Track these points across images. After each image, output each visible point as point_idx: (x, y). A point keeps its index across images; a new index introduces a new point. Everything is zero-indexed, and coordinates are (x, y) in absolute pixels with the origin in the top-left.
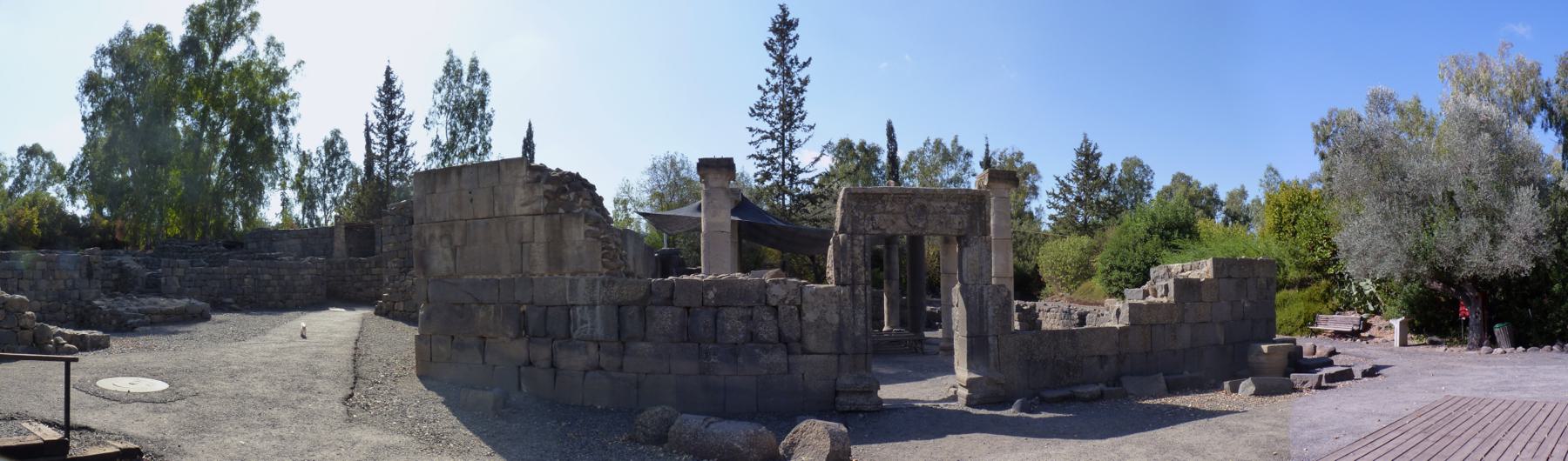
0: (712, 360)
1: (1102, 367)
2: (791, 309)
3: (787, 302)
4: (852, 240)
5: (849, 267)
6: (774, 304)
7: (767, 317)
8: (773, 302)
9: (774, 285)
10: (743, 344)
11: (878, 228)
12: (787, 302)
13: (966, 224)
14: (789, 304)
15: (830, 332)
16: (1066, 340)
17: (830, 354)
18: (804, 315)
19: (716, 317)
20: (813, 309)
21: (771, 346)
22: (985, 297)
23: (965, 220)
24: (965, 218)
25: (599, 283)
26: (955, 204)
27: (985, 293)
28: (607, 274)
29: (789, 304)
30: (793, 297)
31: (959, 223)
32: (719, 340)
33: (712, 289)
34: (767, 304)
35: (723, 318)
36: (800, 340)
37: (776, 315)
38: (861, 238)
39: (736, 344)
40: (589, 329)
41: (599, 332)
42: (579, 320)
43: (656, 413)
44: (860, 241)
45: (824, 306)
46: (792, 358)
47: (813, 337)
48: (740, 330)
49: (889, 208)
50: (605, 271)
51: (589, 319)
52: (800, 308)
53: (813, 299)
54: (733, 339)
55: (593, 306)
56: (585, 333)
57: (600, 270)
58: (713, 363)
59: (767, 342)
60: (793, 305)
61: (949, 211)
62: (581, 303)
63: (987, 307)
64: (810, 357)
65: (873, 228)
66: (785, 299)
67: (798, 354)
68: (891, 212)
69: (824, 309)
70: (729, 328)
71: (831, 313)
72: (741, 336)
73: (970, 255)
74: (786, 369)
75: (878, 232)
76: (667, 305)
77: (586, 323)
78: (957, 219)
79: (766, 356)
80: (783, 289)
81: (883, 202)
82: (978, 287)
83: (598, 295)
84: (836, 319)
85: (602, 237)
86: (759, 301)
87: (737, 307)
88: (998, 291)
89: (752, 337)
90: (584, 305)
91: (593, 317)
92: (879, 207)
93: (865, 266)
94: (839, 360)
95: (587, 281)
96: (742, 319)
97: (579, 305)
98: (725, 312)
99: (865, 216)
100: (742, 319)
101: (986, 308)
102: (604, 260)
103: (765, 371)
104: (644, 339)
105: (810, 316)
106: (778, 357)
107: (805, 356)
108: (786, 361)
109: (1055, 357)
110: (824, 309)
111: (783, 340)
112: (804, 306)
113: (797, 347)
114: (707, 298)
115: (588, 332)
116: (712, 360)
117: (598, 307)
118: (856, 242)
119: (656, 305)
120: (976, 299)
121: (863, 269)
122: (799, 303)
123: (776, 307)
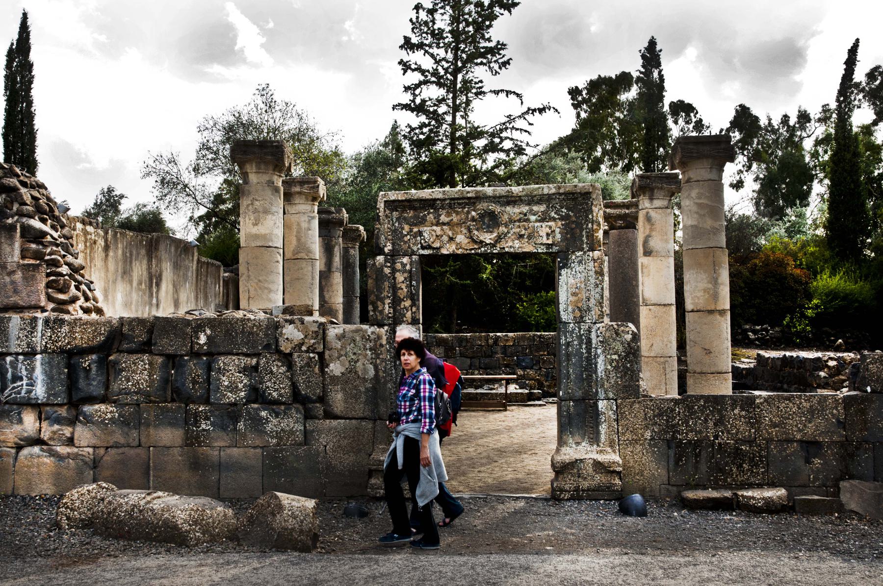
1: (808, 461)
2: (310, 358)
3: (304, 348)
4: (394, 263)
5: (388, 301)
6: (288, 351)
7: (278, 368)
8: (285, 347)
9: (287, 325)
10: (244, 405)
11: (429, 247)
12: (304, 348)
13: (558, 236)
14: (307, 351)
15: (362, 389)
16: (736, 411)
17: (362, 419)
18: (328, 366)
19: (209, 369)
20: (338, 358)
21: (283, 407)
22: (594, 341)
23: (558, 230)
24: (557, 226)
25: (40, 323)
26: (542, 208)
27: (593, 335)
28: (53, 310)
29: (307, 351)
30: (312, 341)
31: (548, 235)
33: (204, 331)
34: (278, 351)
35: (220, 369)
36: (322, 399)
37: (290, 365)
38: (405, 260)
40: (25, 387)
41: (40, 391)
42: (9, 375)
43: (88, 491)
44: (404, 265)
45: (355, 354)
46: (310, 424)
47: (340, 396)
48: (240, 386)
49: (443, 218)
50: (51, 306)
51: (24, 373)
52: (321, 355)
53: (339, 345)
54: (231, 397)
55: (30, 354)
56: (20, 393)
57: (42, 304)
58: (204, 430)
59: (277, 402)
60: (313, 352)
61: (533, 218)
62: (13, 349)
63: (597, 356)
64: (334, 423)
65: (423, 248)
66: (302, 344)
68: (448, 224)
70: (226, 383)
71: (364, 364)
72: (243, 394)
73: (571, 281)
74: (300, 438)
75: (426, 252)
76: (143, 352)
77: (21, 379)
78: (543, 229)
79: (275, 421)
81: (436, 210)
82: (584, 327)
83: (39, 339)
84: (372, 372)
85: (47, 258)
86: (267, 347)
87: (237, 354)
88: (617, 334)
89: (256, 395)
90: (18, 354)
91: (32, 370)
92: (431, 217)
94: (374, 428)
95: (22, 319)
96: (245, 370)
97: (10, 354)
98: (222, 361)
99: (411, 231)
100: (245, 370)
101: (595, 358)
102: (50, 290)
103: (275, 441)
104: (104, 400)
105: (336, 368)
106: (292, 423)
108: (302, 428)
109: (716, 437)
111: (297, 397)
112: (327, 353)
113: (319, 409)
114: (199, 344)
115: (23, 392)
116: (204, 426)
117: (38, 357)
118: (398, 266)
119: (131, 352)
120: (580, 344)
121: (408, 303)
122: (320, 348)
123: (291, 354)
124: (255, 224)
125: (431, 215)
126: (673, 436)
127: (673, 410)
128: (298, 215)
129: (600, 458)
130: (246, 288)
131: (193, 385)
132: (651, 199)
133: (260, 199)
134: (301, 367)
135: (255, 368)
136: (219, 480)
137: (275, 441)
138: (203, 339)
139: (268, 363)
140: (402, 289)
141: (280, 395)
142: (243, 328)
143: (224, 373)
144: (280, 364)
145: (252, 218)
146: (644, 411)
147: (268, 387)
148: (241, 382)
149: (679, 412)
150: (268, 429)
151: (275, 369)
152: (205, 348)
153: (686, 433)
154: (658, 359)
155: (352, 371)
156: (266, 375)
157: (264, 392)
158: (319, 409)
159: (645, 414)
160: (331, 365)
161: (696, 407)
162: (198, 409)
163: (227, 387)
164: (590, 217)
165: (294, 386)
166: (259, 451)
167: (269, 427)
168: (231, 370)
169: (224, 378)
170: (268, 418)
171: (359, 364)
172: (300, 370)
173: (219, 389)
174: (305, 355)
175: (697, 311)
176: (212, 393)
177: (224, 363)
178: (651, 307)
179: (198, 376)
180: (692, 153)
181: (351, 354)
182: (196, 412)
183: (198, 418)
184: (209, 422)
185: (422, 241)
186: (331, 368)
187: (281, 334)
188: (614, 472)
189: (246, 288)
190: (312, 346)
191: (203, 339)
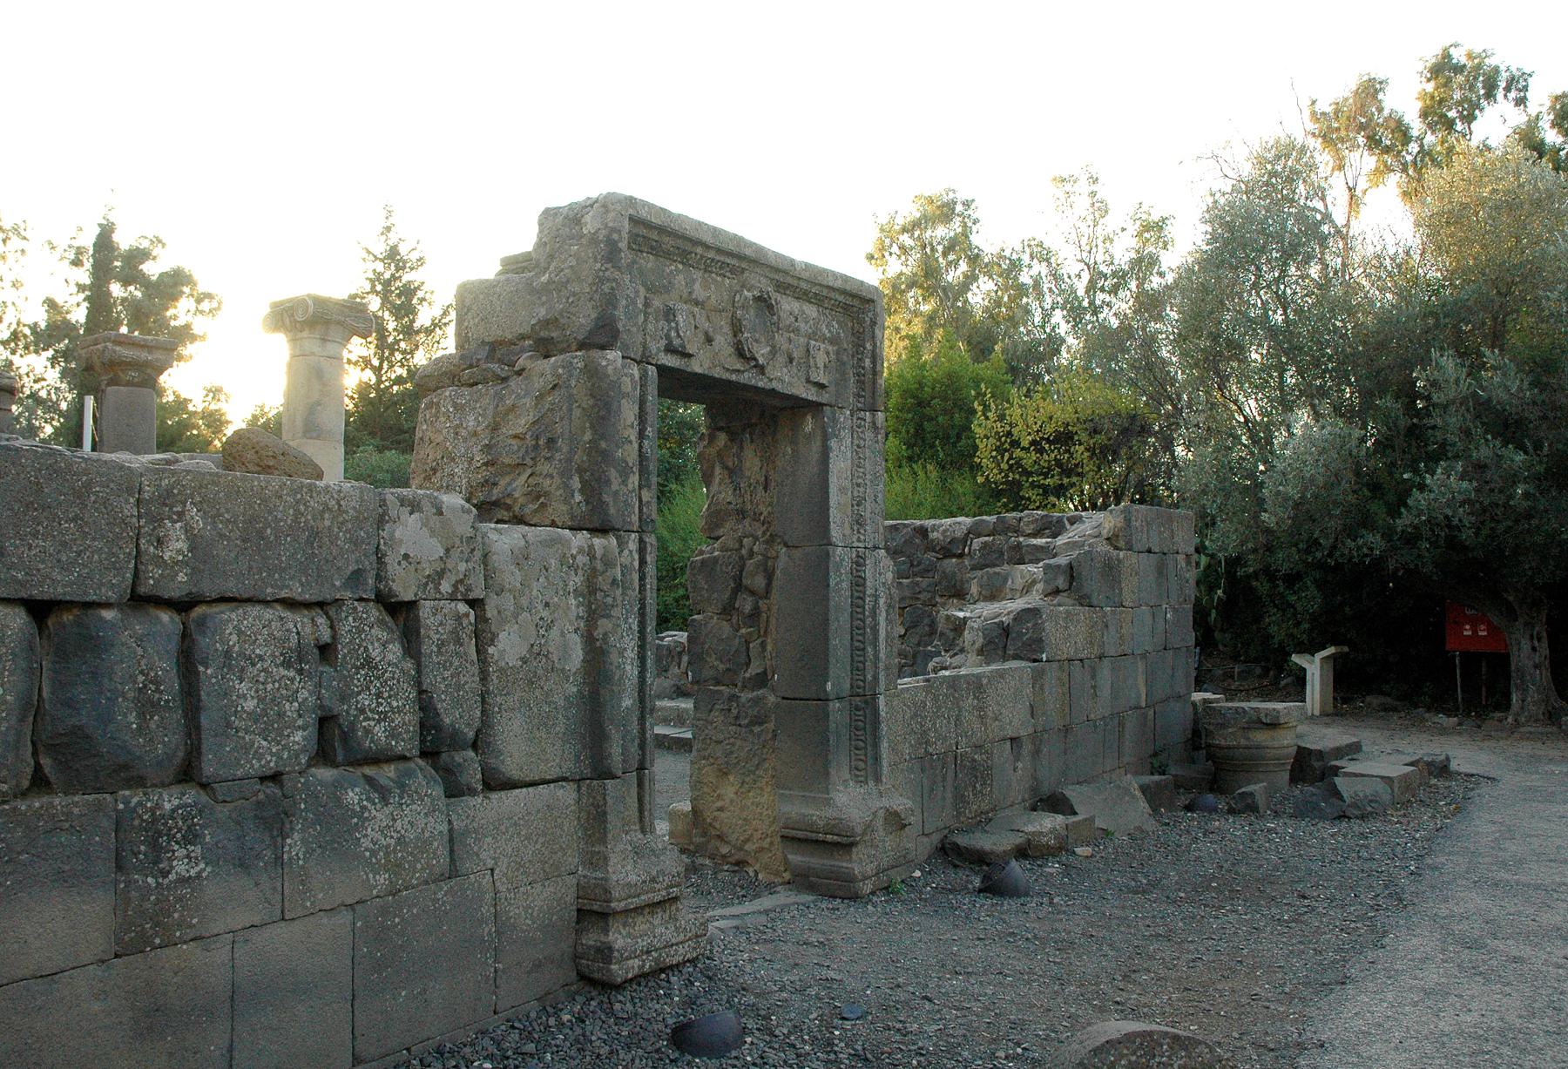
0: (180, 868)
2: (459, 618)
3: (446, 587)
12: (446, 587)
18: (494, 637)
29: (452, 598)
30: (462, 567)
32: (209, 767)
35: (227, 654)
37: (410, 637)
39: (275, 777)
48: (290, 709)
65: (670, 349)
66: (441, 574)
67: (472, 792)
69: (545, 614)
70: (250, 705)
72: (298, 736)
79: (380, 815)
80: (433, 533)
86: (356, 577)
93: (643, 471)
96: (295, 659)
100: (295, 659)
103: (383, 878)
107: (494, 796)
108: (444, 827)
110: (545, 614)
113: (470, 765)
114: (159, 561)
116: (180, 868)
125: (681, 277)
131: (141, 715)
134: (441, 644)
135: (326, 651)
136: (231, 1049)
137: (383, 878)
138: (177, 545)
139: (360, 631)
140: (631, 442)
141: (393, 734)
142: (298, 513)
143: (243, 670)
144: (384, 635)
147: (362, 711)
148: (292, 699)
150: (366, 843)
151: (375, 653)
152: (182, 577)
155: (537, 653)
156: (358, 668)
157: (352, 725)
160: (503, 635)
162: (158, 806)
163: (254, 717)
164: (868, 346)
165: (425, 704)
166: (345, 918)
167: (370, 837)
168: (261, 658)
169: (243, 687)
170: (364, 808)
171: (554, 633)
172: (439, 653)
173: (229, 725)
174: (448, 606)
176: (208, 742)
177: (240, 633)
179: (156, 682)
181: (540, 607)
182: (155, 820)
183: (163, 840)
184: (197, 850)
185: (673, 334)
186: (501, 646)
187: (393, 542)
190: (461, 581)
191: (177, 545)
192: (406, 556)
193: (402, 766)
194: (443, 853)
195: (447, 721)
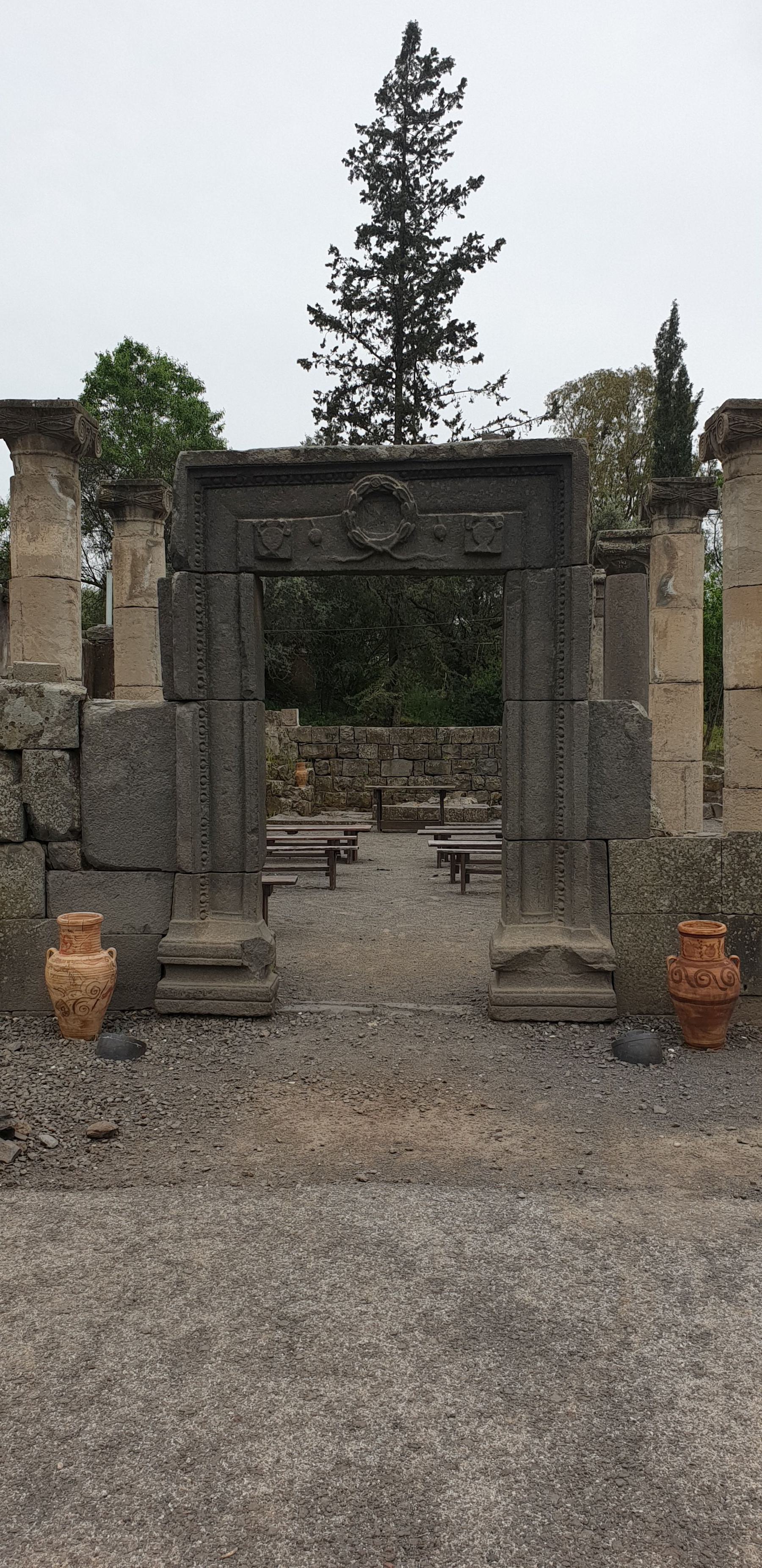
2: (55, 761)
3: (43, 741)
29: (50, 748)
36: (76, 834)
52: (75, 753)
108: (41, 886)
124: (31, 540)
126: (710, 905)
127: (711, 860)
128: (132, 539)
129: (580, 946)
130: (19, 645)
132: (672, 519)
133: (38, 497)
134: (38, 776)
145: (27, 530)
146: (658, 860)
149: (722, 863)
153: (735, 903)
154: (675, 765)
158: (70, 850)
159: (661, 867)
161: (754, 855)
172: (36, 781)
175: (744, 688)
178: (666, 686)
180: (744, 427)
188: (601, 971)
189: (19, 645)
192: (13, 723)
193: (13, 847)
194: (39, 900)
195: (42, 822)
